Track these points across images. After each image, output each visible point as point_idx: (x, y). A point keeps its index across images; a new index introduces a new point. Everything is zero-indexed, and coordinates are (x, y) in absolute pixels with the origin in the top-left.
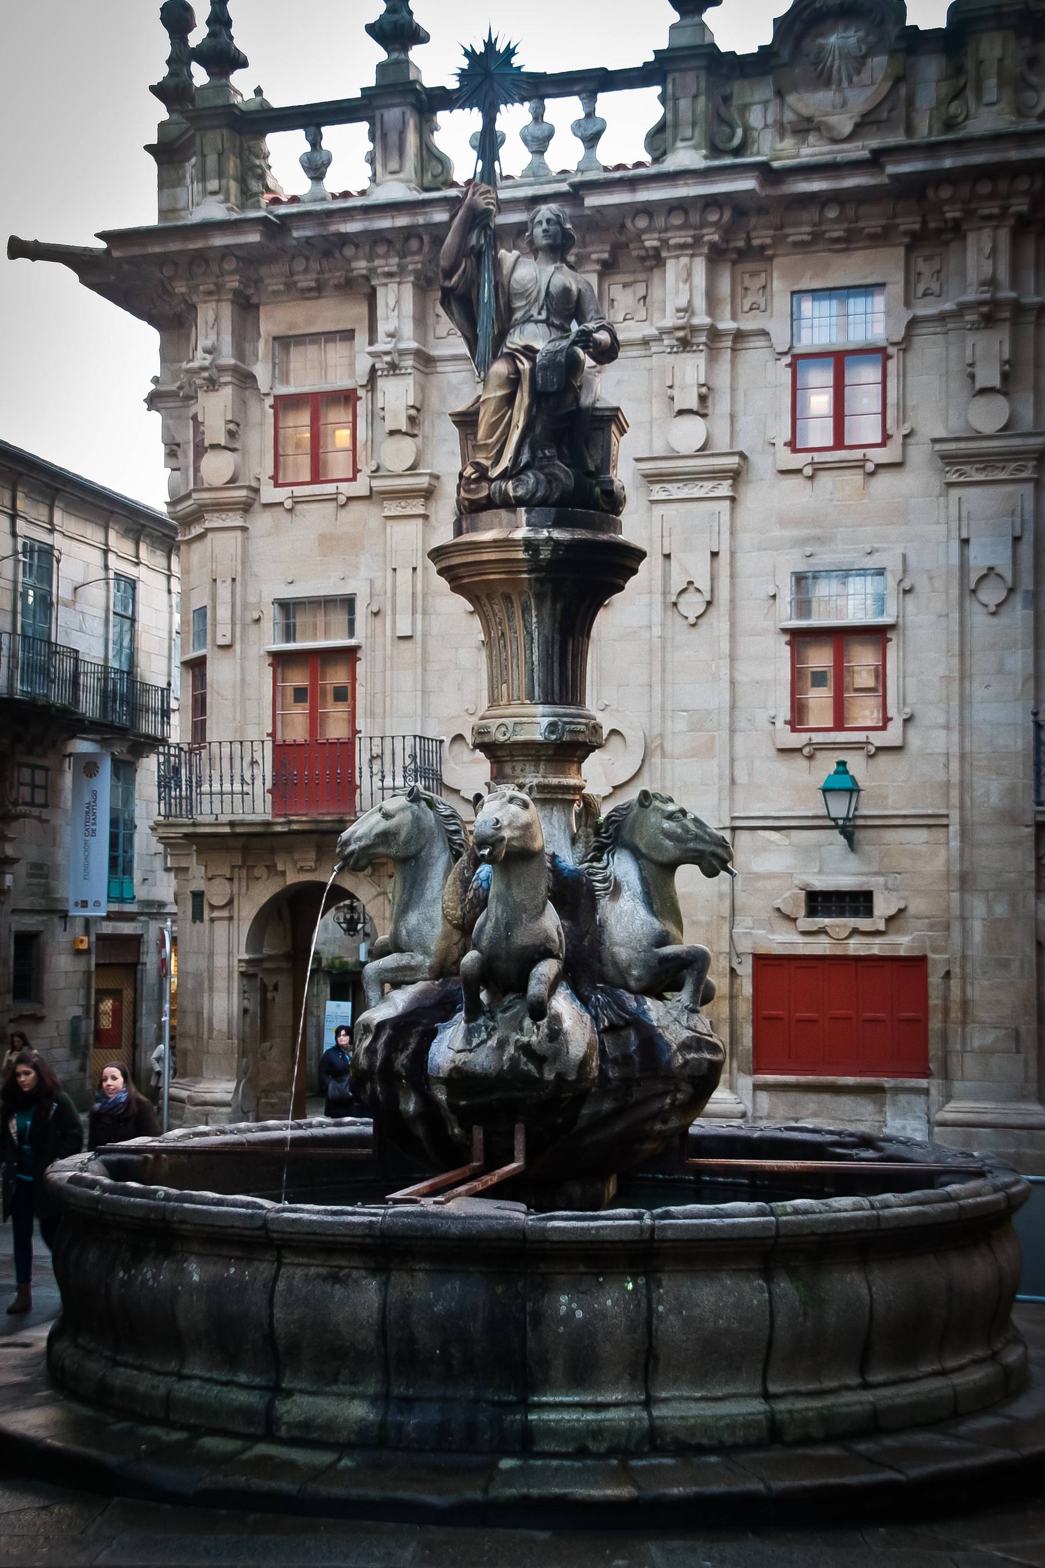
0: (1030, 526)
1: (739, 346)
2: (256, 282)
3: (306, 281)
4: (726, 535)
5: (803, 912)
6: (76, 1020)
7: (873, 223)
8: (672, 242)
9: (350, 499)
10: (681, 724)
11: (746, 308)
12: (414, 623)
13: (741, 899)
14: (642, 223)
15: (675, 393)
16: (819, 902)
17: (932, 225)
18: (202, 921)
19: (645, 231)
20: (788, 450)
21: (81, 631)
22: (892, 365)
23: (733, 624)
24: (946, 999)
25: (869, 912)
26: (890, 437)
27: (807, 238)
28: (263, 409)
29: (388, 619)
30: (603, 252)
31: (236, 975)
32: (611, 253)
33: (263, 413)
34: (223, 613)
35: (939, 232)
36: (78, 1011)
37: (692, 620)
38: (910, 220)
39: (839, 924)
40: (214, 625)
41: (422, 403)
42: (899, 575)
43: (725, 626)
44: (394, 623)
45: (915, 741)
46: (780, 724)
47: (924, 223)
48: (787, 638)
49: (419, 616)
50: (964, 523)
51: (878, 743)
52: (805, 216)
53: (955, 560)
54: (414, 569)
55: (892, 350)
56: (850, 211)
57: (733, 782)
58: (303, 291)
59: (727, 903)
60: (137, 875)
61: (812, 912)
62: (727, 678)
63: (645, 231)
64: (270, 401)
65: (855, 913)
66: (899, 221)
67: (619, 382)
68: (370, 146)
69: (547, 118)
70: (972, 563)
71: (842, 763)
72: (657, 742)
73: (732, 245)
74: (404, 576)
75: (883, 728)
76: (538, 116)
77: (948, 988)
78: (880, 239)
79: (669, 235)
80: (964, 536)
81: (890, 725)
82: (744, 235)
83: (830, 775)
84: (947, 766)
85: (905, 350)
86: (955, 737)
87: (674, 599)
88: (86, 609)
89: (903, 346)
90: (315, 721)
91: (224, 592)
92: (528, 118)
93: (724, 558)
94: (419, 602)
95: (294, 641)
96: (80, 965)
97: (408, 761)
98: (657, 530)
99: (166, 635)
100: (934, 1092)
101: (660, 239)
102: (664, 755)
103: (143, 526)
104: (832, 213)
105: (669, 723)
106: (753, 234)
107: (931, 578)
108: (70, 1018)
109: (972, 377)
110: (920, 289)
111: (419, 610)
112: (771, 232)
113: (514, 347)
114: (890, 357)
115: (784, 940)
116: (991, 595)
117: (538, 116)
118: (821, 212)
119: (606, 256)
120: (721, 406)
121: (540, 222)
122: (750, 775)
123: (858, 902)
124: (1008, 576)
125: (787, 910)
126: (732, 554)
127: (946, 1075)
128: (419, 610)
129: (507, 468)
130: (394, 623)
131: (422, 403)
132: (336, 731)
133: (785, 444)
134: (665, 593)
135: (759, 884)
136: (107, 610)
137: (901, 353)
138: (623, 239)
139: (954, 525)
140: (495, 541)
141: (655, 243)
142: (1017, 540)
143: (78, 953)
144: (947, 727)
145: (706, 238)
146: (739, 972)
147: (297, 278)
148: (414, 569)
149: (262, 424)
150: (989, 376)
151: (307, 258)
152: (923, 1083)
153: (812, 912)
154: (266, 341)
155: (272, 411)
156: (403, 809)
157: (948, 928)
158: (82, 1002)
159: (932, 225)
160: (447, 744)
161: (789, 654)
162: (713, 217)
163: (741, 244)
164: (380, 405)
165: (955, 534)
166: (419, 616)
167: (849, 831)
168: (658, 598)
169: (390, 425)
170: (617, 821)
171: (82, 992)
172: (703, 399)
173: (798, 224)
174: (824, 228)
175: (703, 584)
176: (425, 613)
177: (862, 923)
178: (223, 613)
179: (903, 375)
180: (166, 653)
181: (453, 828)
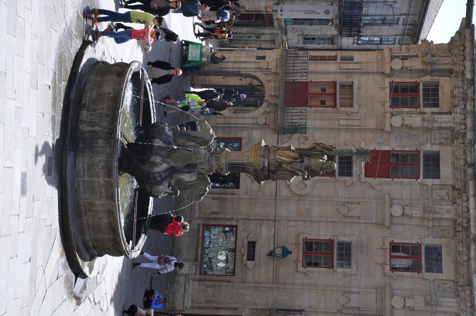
0: (362, 313)
1: (425, 227)
2: (457, 76)
3: (456, 92)
4: (364, 221)
5: (249, 240)
6: (245, 8)
7: (461, 271)
8: (458, 208)
10: (307, 206)
11: (438, 230)
12: (343, 125)
13: (255, 222)
14: (465, 199)
15: (410, 208)
16: (252, 245)
18: (256, 59)
19: (462, 200)
20: (390, 241)
21: (376, 7)
23: (337, 222)
24: (222, 281)
25: (248, 259)
27: (458, 250)
28: (416, 78)
31: (239, 70)
32: (457, 189)
33: (414, 78)
34: (350, 66)
35: (458, 291)
36: (247, 8)
37: (339, 210)
38: (462, 282)
39: (245, 251)
40: (347, 63)
41: (413, 129)
43: (336, 220)
44: (343, 119)
45: (298, 275)
46: (306, 235)
47: (460, 286)
48: (332, 238)
49: (345, 127)
50: (364, 293)
51: (298, 264)
52: (465, 249)
53: (353, 290)
54: (360, 126)
55: (421, 274)
56: (465, 263)
57: (289, 221)
58: (453, 91)
59: (253, 218)
60: (295, 26)
61: (249, 243)
62: (320, 220)
63: (462, 200)
64: (418, 80)
65: (248, 256)
66: (462, 278)
67: (416, 190)
70: (352, 295)
71: (291, 253)
72: (302, 199)
73: (457, 226)
74: (357, 123)
77: (225, 282)
78: (457, 272)
79: (460, 207)
81: (304, 268)
82: (460, 230)
84: (291, 284)
86: (299, 287)
87: (346, 205)
88: (384, 9)
90: (315, 95)
91: (356, 66)
93: (358, 221)
94: (349, 127)
95: (340, 89)
96: (263, 9)
97: (298, 124)
98: (367, 200)
99: (380, 34)
100: (195, 276)
101: (459, 204)
102: (298, 200)
103: (417, 27)
104: (465, 258)
105: (308, 202)
106: (460, 233)
107: (348, 282)
108: (245, 5)
111: (347, 127)
112: (461, 239)
115: (242, 234)
116: (342, 300)
118: (466, 255)
119: (456, 187)
120: (406, 221)
122: (291, 226)
123: (251, 257)
124: (347, 305)
125: (250, 236)
126: (359, 223)
127: (200, 280)
128: (347, 127)
130: (343, 119)
131: (413, 129)
132: (312, 102)
133: (392, 241)
134: (348, 203)
135: (258, 228)
136: (385, 15)
138: (461, 192)
139: (364, 290)
141: (458, 203)
143: (266, 8)
144: (302, 285)
145: (458, 218)
146: (233, 221)
147: (457, 89)
148: (360, 126)
149: (411, 78)
150: (409, 303)
151: (463, 93)
152: (198, 273)
153: (249, 243)
154: (437, 79)
155: (415, 81)
157: (242, 282)
158: (250, 10)
160: (304, 135)
161: (327, 239)
162: (465, 221)
163: (457, 229)
164: (412, 116)
165: (361, 290)
166: (345, 127)
167: (271, 254)
168: (346, 200)
169: (406, 119)
171: (254, 10)
172: (408, 215)
173: (462, 247)
174: (461, 255)
175: (349, 214)
176: (346, 129)
177: (245, 258)
178: (350, 66)
180: (374, 34)
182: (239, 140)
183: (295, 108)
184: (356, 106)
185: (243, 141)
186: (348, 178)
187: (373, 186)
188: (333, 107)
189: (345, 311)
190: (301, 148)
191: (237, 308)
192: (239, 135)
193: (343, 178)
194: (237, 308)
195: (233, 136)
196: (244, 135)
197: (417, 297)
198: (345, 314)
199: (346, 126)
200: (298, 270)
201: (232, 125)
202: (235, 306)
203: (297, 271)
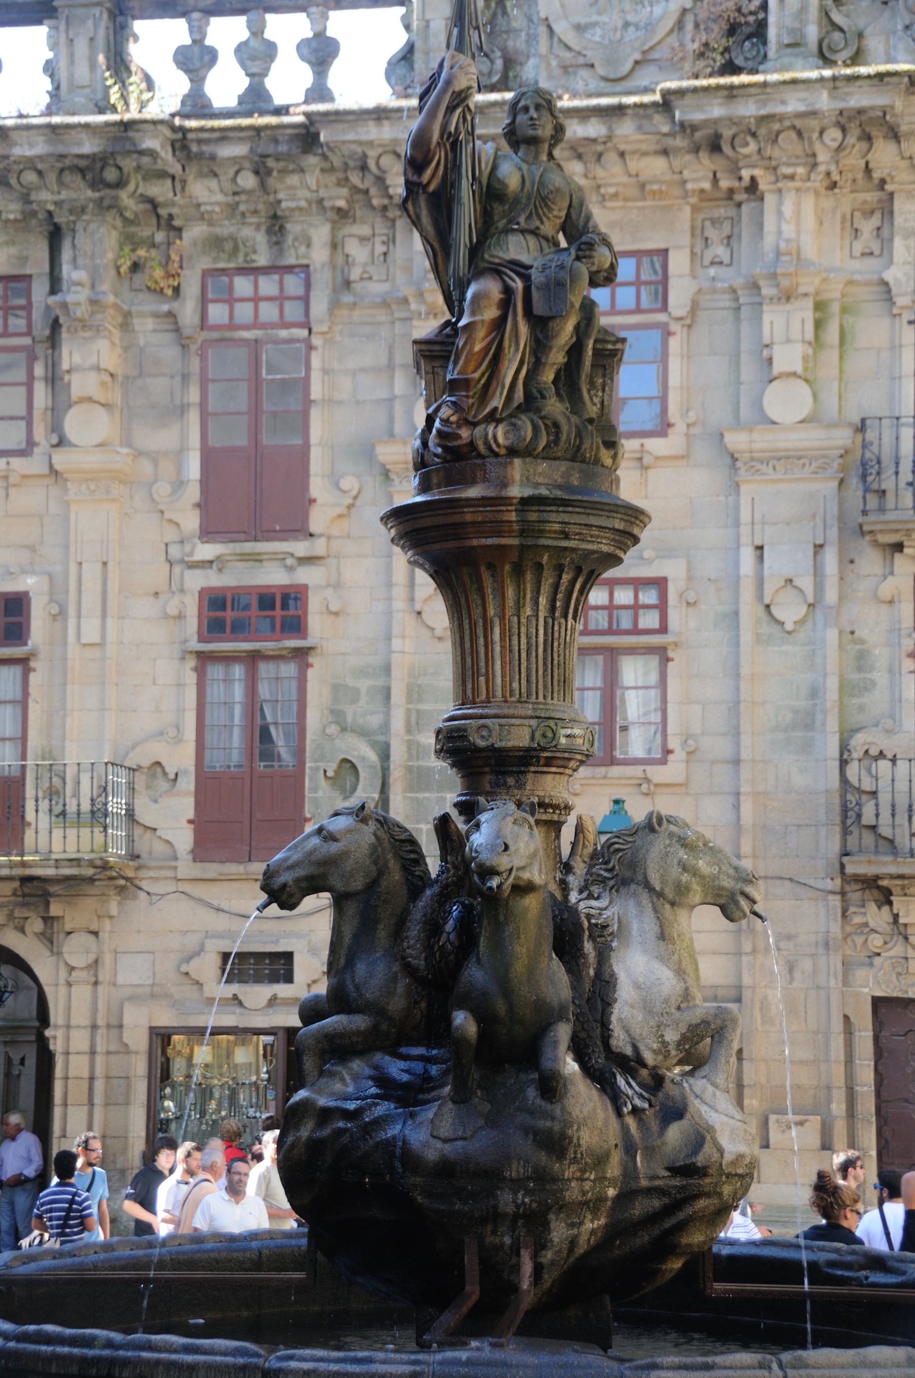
9: (24, 477)
17: (725, 184)
22: (674, 344)
26: (669, 425)
29: (72, 622)
30: (339, 197)
35: (731, 191)
42: (682, 585)
47: (715, 180)
49: (110, 622)
50: (758, 527)
51: (656, 780)
54: (105, 564)
55: (674, 327)
68: (50, 55)
69: (268, 35)
74: (91, 573)
75: (663, 761)
76: (257, 30)
80: (758, 542)
83: (605, 817)
84: (737, 807)
85: (689, 327)
87: (418, 607)
89: (688, 321)
92: (245, 35)
109: (770, 360)
110: (708, 256)
113: (497, 261)
114: (669, 334)
117: (257, 30)
119: (341, 203)
121: (526, 109)
129: (496, 409)
137: (685, 329)
140: (484, 498)
142: (818, 548)
148: (105, 564)
156: (349, 831)
159: (725, 184)
170: (619, 850)
179: (688, 356)
181: (412, 856)
182: (161, 1038)
183: (30, 816)
184: (28, 583)
185: (165, 1019)
186: (314, 604)
187: (342, 510)
188: (27, 671)
189: (831, 595)
190: (192, 787)
191: (846, 1017)
192: (138, 1040)
193: (316, 623)
194: (846, 1017)
195: (140, 1066)
196: (137, 1023)
197: (766, 330)
198: (841, 598)
199: (104, 616)
200: (680, 779)
201: (99, 1071)
202: (837, 1025)
203: (685, 785)
